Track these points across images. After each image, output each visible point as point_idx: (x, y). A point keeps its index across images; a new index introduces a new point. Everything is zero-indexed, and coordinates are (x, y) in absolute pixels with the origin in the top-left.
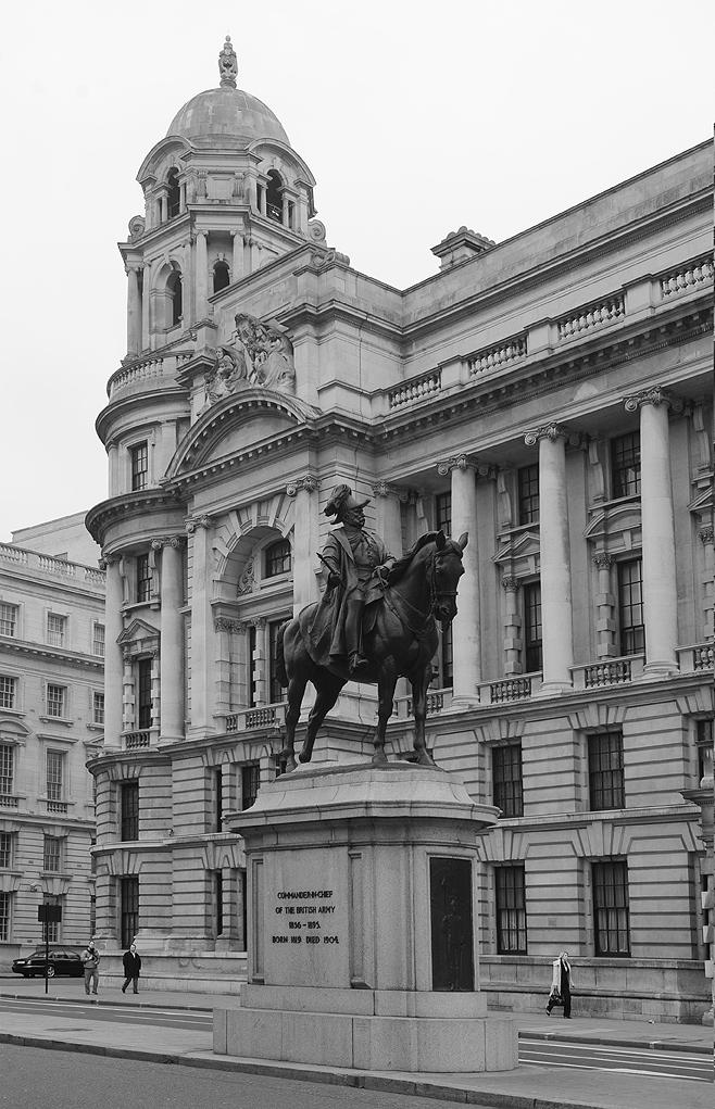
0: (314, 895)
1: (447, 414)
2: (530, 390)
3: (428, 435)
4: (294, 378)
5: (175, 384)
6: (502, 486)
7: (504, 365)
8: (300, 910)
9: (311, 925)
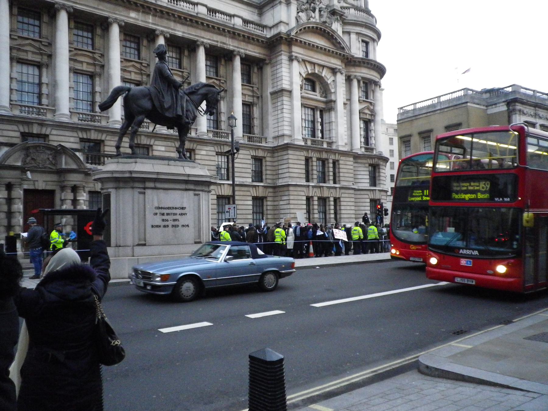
0: (176, 208)
8: (168, 214)
9: (174, 220)
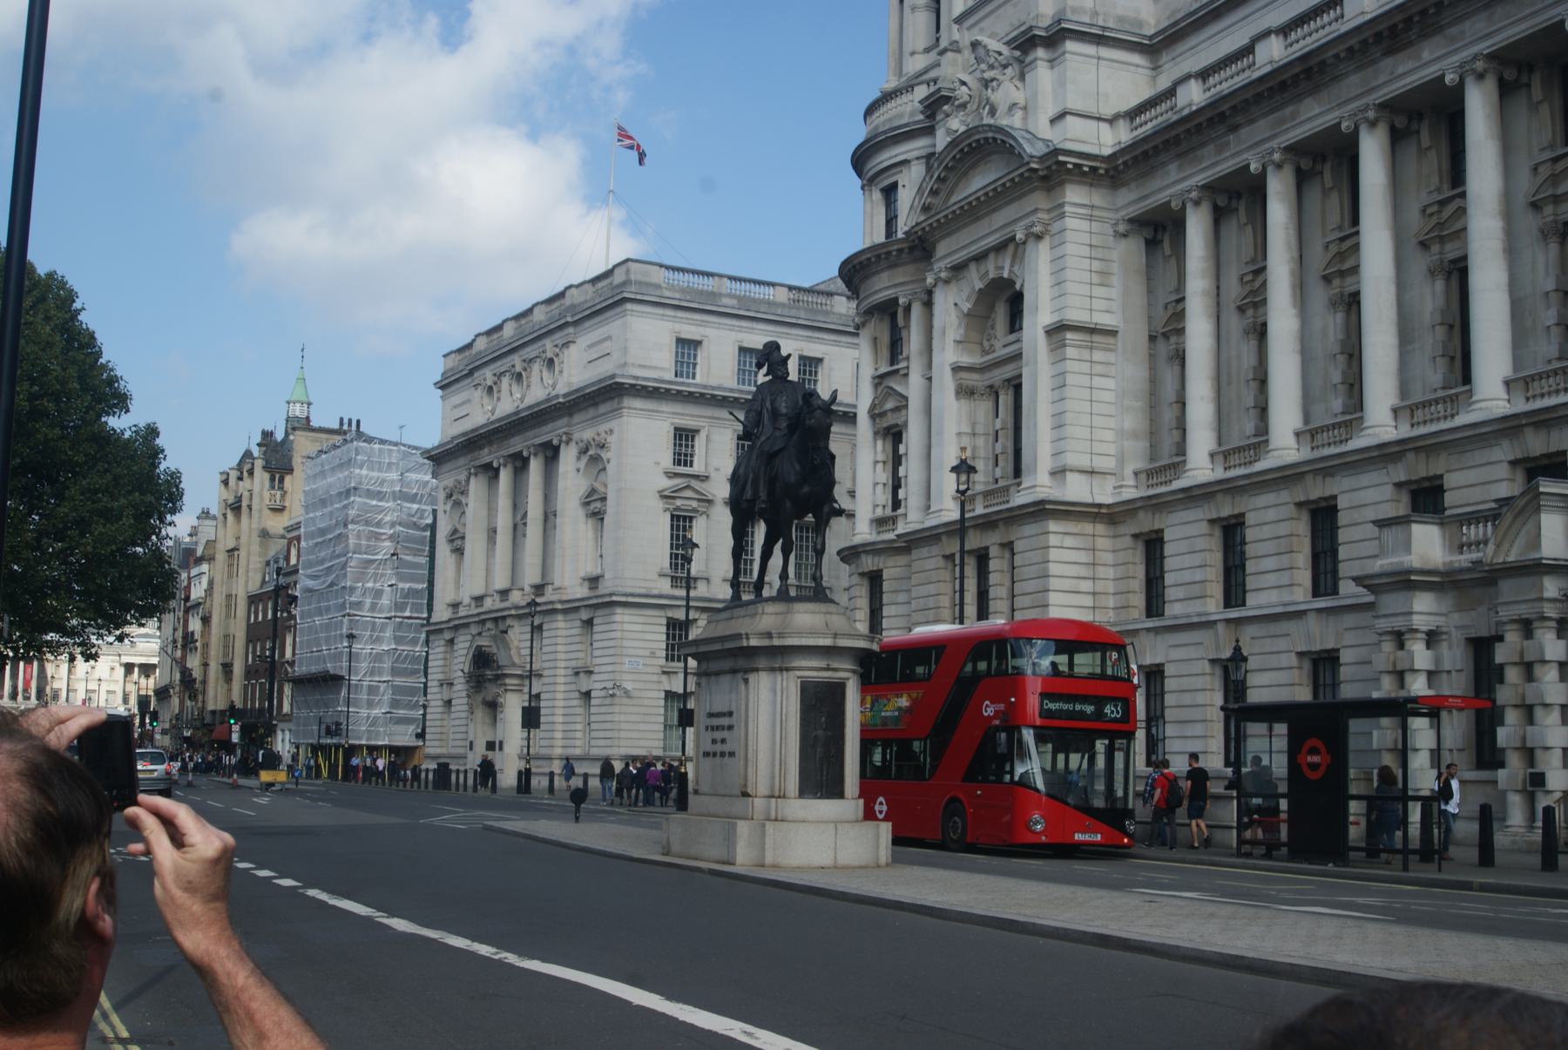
3: (1163, 164)
5: (921, 117)
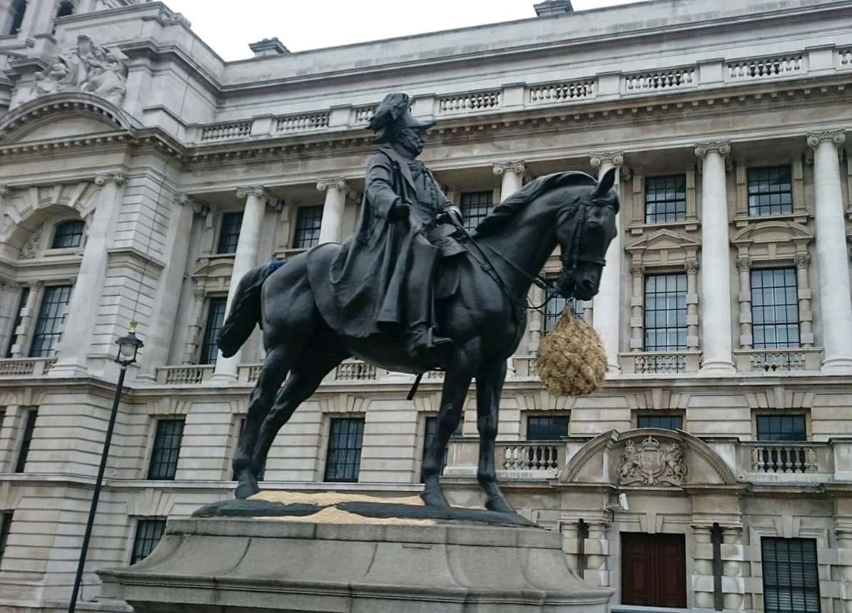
1: (254, 153)
2: (328, 151)
3: (233, 166)
4: (124, 95)
6: (285, 215)
7: (304, 129)
